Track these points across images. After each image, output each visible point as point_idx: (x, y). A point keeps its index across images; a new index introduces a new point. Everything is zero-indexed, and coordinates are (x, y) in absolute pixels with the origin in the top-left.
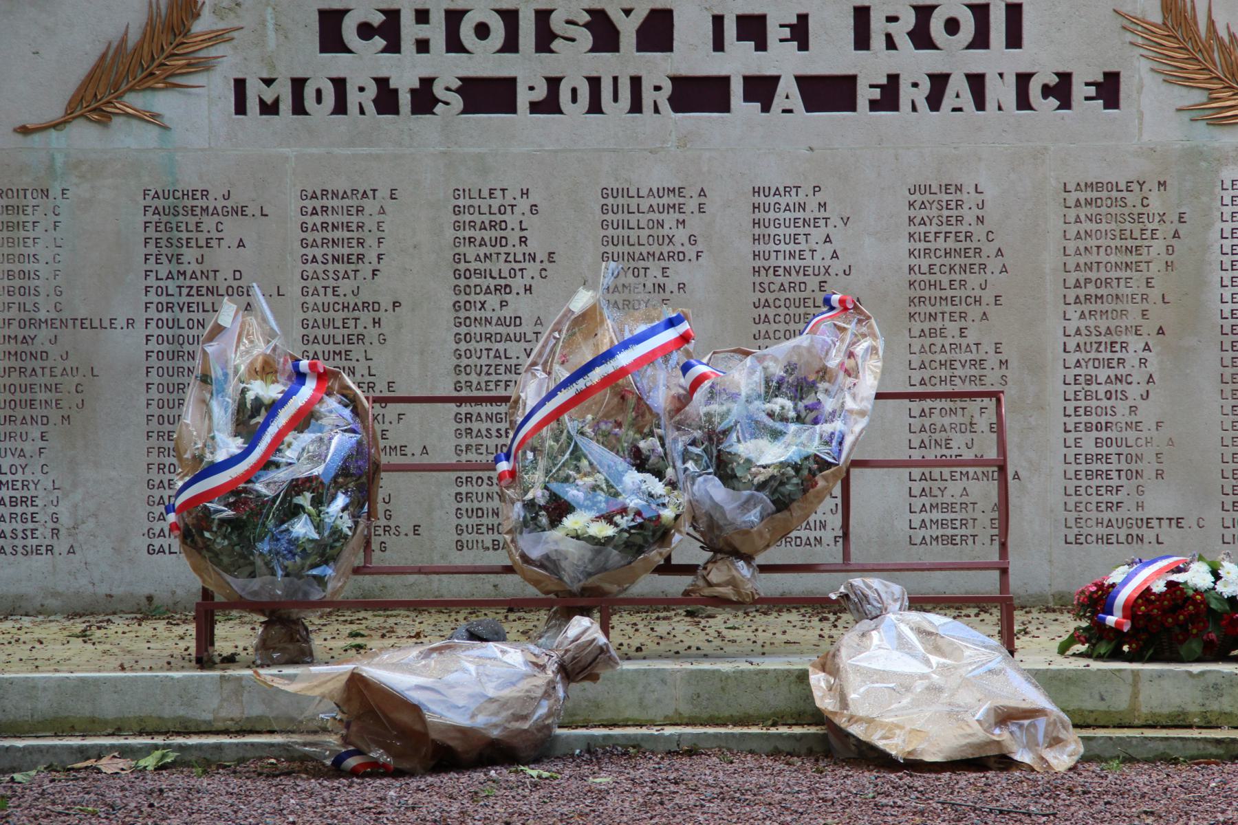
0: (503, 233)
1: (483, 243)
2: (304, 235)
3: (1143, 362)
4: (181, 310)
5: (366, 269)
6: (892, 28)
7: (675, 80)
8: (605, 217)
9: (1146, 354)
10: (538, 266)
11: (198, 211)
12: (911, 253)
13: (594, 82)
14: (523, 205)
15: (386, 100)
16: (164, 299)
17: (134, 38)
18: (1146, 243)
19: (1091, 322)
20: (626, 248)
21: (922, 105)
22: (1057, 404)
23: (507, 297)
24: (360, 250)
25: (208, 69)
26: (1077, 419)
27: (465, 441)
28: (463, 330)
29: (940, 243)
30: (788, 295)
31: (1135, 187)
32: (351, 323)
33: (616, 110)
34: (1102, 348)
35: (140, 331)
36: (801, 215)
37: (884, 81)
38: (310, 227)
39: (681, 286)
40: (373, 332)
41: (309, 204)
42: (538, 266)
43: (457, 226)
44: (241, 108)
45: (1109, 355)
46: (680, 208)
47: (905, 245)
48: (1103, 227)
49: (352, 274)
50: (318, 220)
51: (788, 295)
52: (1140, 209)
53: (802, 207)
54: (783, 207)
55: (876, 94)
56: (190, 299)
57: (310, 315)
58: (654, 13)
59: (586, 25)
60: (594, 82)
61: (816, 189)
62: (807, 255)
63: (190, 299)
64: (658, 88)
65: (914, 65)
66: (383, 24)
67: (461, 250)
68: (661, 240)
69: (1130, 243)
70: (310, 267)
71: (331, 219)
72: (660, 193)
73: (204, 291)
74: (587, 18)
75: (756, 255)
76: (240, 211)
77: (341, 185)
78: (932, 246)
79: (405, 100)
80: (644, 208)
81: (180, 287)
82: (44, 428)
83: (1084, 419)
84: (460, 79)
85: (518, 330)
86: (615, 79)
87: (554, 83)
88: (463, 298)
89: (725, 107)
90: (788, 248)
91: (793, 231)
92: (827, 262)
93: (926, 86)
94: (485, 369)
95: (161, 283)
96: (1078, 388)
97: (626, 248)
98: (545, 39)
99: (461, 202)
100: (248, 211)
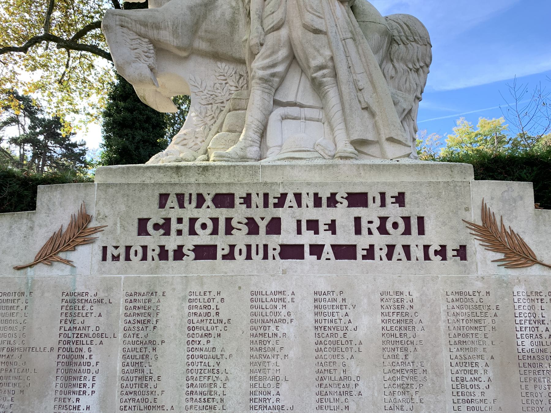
0: (209, 311)
1: (200, 315)
2: (126, 311)
3: (485, 372)
4: (73, 344)
5: (151, 326)
6: (370, 226)
7: (281, 246)
8: (252, 304)
9: (487, 368)
10: (223, 325)
11: (84, 301)
12: (383, 321)
13: (249, 247)
14: (218, 298)
15: (163, 254)
16: (67, 339)
17: (64, 230)
18: (483, 318)
19: (462, 353)
20: (261, 318)
21: (385, 258)
22: (449, 390)
23: (210, 339)
24: (149, 318)
25: (92, 243)
26: (458, 398)
27: (189, 404)
28: (191, 353)
29: (395, 317)
30: (330, 339)
31: (477, 294)
32: (144, 350)
33: (257, 258)
34: (467, 365)
35: (55, 354)
36: (335, 303)
37: (368, 247)
38: (129, 308)
39: (284, 335)
40: (152, 354)
41: (129, 298)
42: (223, 325)
43: (190, 308)
44: (104, 258)
45: (470, 368)
46: (283, 300)
47: (379, 318)
48: (464, 311)
49: (145, 328)
50: (132, 305)
51: (330, 339)
52: (479, 303)
53: (335, 300)
54: (327, 300)
55: (365, 253)
56: (77, 339)
57: (127, 346)
58: (273, 219)
59: (246, 224)
60: (249, 247)
61: (341, 292)
62: (338, 321)
63: (77, 339)
64: (274, 249)
65: (379, 241)
66: (164, 224)
67: (191, 318)
68: (276, 314)
69: (476, 318)
70: (127, 325)
71: (137, 304)
72: (275, 293)
73: (83, 335)
74: (246, 221)
75: (316, 321)
76: (100, 301)
77: (143, 290)
78: (392, 318)
79: (171, 254)
80: (269, 300)
81: (74, 334)
82: (13, 396)
83: (461, 397)
84: (194, 246)
85: (214, 353)
86: (257, 245)
87: (232, 247)
88: (191, 339)
89: (302, 258)
90: (330, 318)
91: (331, 311)
92: (347, 325)
93: (385, 250)
94: (199, 371)
95: (67, 332)
96: (458, 383)
97: (261, 318)
98: (229, 230)
99: (192, 297)
100: (104, 301)
